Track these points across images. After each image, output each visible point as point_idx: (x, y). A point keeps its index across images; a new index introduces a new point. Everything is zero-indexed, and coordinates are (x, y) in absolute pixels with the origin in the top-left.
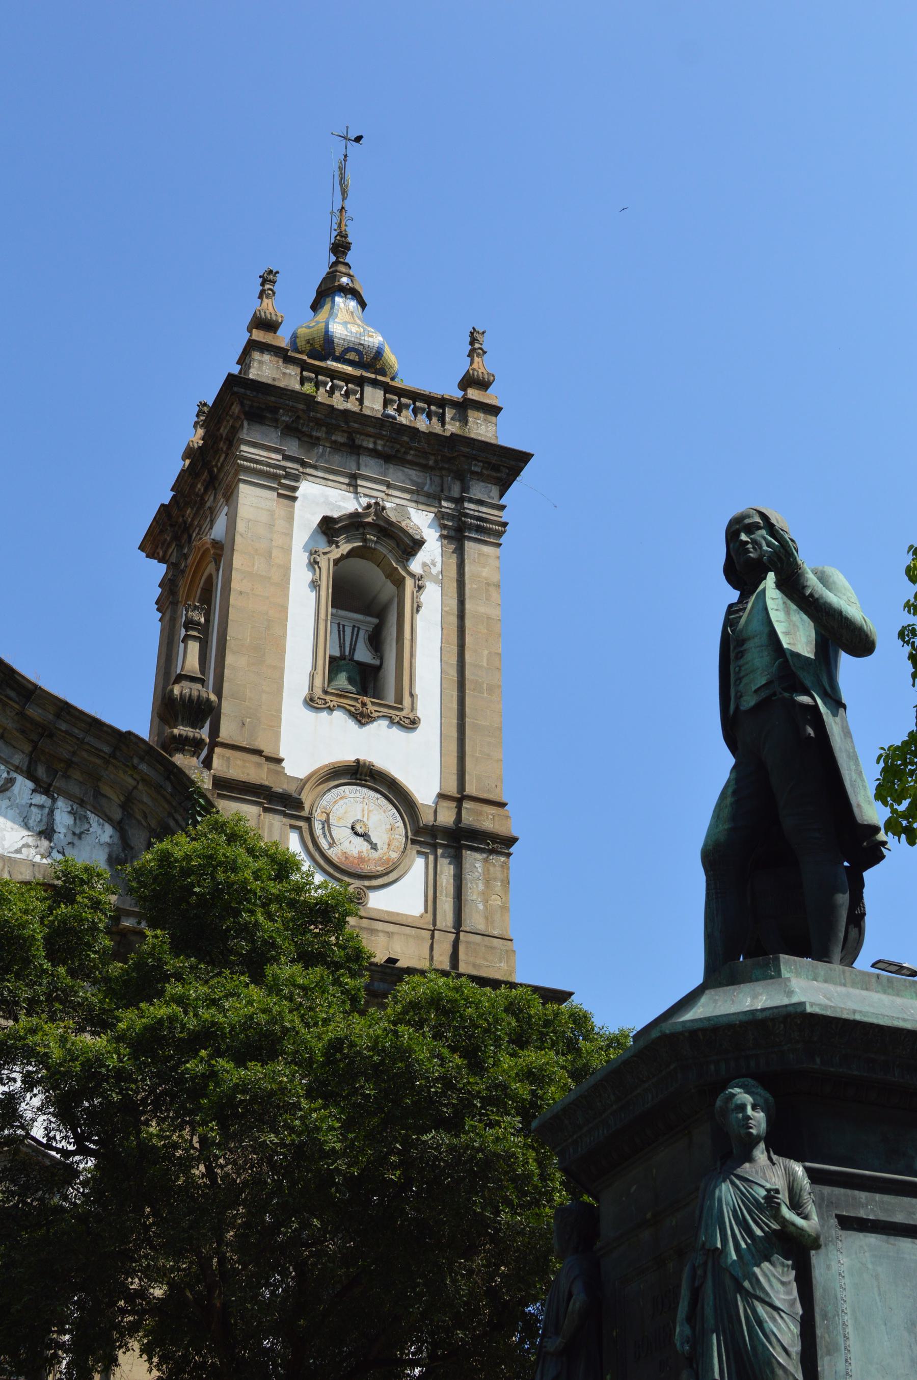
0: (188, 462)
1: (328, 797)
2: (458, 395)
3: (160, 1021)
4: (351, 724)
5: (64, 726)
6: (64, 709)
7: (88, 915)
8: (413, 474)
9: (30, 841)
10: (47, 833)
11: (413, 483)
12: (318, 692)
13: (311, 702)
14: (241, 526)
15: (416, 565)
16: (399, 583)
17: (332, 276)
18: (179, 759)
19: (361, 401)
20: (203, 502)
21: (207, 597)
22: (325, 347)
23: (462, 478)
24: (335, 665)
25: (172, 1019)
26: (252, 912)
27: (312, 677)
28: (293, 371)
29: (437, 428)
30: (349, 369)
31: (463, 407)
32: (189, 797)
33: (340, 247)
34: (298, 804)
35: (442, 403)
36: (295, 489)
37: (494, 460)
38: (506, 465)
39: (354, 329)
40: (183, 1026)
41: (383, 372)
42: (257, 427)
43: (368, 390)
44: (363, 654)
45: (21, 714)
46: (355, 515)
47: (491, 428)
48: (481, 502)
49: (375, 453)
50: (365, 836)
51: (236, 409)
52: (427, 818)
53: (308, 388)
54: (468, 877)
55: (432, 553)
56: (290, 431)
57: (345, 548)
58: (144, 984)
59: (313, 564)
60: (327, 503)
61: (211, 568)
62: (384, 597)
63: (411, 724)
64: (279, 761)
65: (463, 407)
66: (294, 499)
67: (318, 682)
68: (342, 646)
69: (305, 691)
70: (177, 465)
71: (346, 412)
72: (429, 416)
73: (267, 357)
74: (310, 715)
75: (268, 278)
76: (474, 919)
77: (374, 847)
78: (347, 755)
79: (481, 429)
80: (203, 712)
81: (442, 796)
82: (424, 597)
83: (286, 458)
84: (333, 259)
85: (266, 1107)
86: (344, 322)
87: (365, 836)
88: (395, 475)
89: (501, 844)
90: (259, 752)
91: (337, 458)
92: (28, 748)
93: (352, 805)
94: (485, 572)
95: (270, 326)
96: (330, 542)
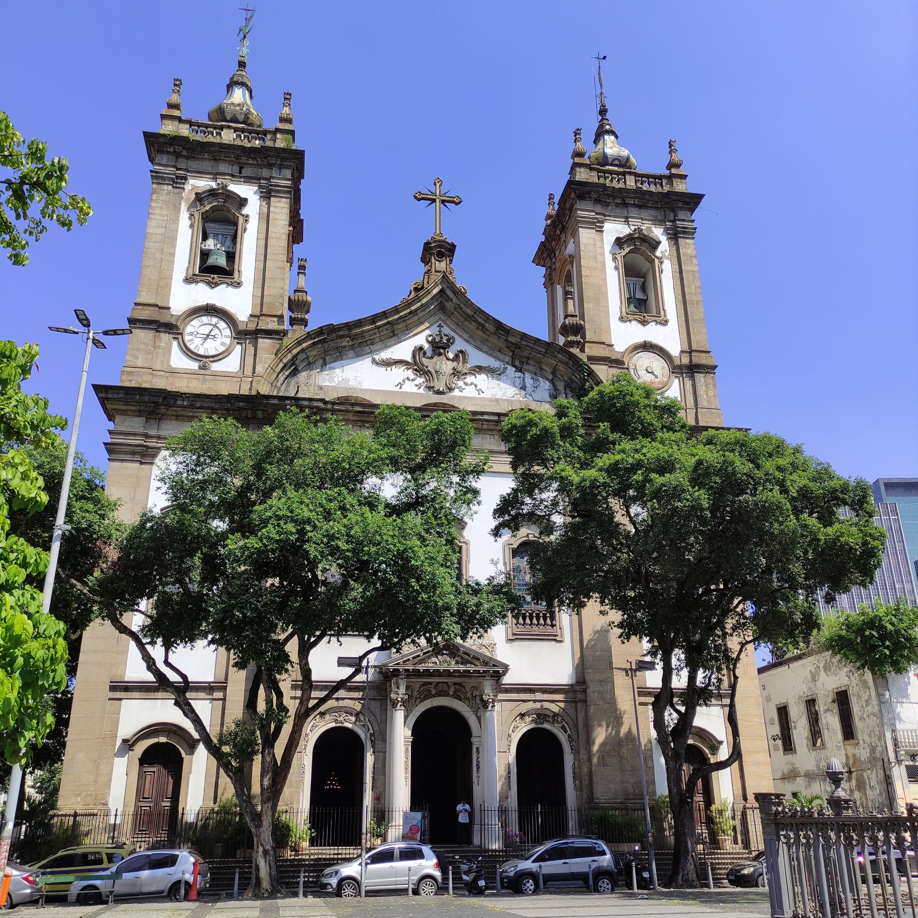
0: (549, 222)
1: (634, 358)
2: (667, 172)
3: (618, 461)
4: (640, 326)
5: (524, 343)
6: (524, 336)
7: (574, 421)
8: (652, 212)
9: (517, 392)
10: (523, 388)
11: (653, 216)
12: (624, 314)
13: (622, 319)
14: (582, 247)
15: (658, 253)
16: (652, 262)
17: (601, 126)
18: (571, 350)
19: (625, 183)
20: (560, 238)
21: (569, 279)
22: (604, 160)
23: (673, 210)
24: (630, 300)
25: (623, 459)
26: (640, 412)
27: (621, 308)
28: (594, 174)
29: (660, 190)
30: (616, 168)
31: (670, 177)
32: (580, 366)
33: (603, 112)
34: (622, 363)
35: (661, 177)
36: (602, 227)
37: (688, 200)
38: (693, 201)
39: (615, 149)
40: (627, 462)
41: (630, 167)
42: (582, 202)
43: (628, 177)
44: (639, 295)
45: (507, 341)
46: (630, 234)
47: (684, 185)
48: (683, 220)
49: (634, 205)
50: (652, 373)
51: (573, 195)
52: (677, 362)
53: (602, 181)
54: (698, 385)
55: (665, 246)
56: (597, 201)
57: (627, 250)
58: (601, 446)
59: (615, 259)
60: (617, 231)
61: (569, 267)
62: (645, 269)
63: (665, 323)
64: (612, 346)
65: (670, 177)
66: (602, 231)
67: (624, 310)
68: (630, 293)
69: (619, 315)
70: (543, 224)
71: (620, 188)
72: (655, 184)
73: (582, 169)
74: (623, 324)
75: (577, 133)
76: (703, 402)
77: (656, 377)
78: (641, 340)
79: (680, 187)
80: (578, 329)
81: (682, 352)
82: (664, 266)
83: (597, 214)
84: (600, 118)
85: (676, 492)
86: (611, 147)
87: (652, 373)
88: (644, 213)
89: (710, 369)
90: (603, 343)
91: (618, 210)
92: (511, 354)
93: (645, 360)
94: (689, 251)
95: (580, 154)
96: (621, 248)
